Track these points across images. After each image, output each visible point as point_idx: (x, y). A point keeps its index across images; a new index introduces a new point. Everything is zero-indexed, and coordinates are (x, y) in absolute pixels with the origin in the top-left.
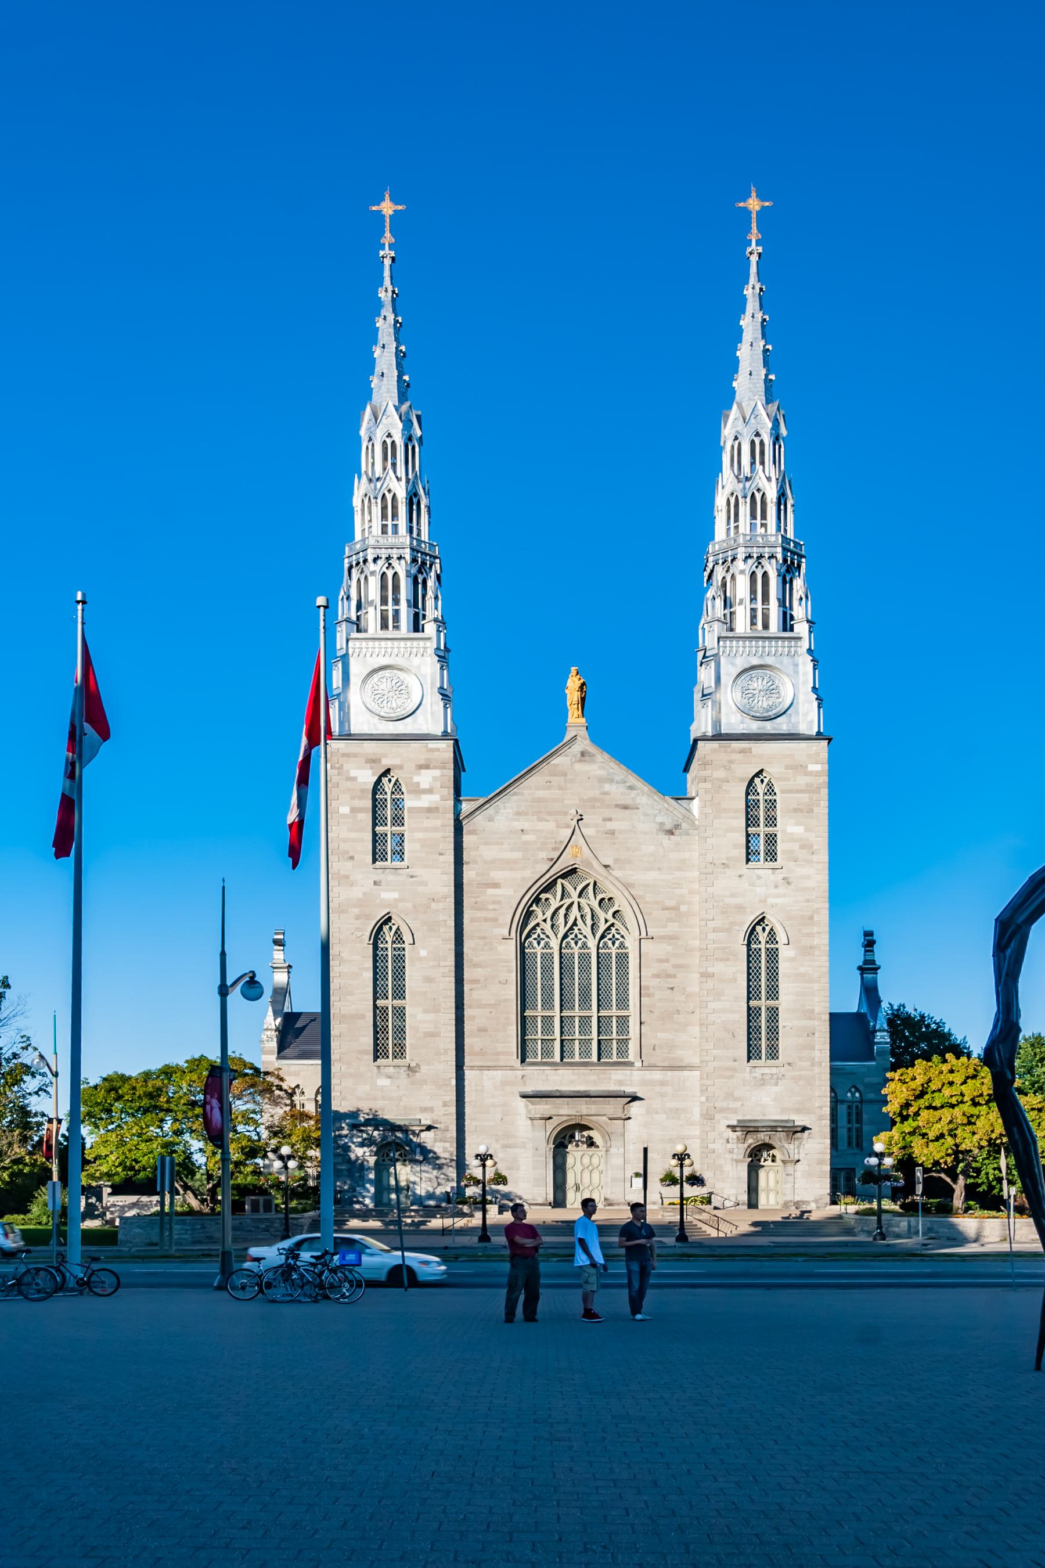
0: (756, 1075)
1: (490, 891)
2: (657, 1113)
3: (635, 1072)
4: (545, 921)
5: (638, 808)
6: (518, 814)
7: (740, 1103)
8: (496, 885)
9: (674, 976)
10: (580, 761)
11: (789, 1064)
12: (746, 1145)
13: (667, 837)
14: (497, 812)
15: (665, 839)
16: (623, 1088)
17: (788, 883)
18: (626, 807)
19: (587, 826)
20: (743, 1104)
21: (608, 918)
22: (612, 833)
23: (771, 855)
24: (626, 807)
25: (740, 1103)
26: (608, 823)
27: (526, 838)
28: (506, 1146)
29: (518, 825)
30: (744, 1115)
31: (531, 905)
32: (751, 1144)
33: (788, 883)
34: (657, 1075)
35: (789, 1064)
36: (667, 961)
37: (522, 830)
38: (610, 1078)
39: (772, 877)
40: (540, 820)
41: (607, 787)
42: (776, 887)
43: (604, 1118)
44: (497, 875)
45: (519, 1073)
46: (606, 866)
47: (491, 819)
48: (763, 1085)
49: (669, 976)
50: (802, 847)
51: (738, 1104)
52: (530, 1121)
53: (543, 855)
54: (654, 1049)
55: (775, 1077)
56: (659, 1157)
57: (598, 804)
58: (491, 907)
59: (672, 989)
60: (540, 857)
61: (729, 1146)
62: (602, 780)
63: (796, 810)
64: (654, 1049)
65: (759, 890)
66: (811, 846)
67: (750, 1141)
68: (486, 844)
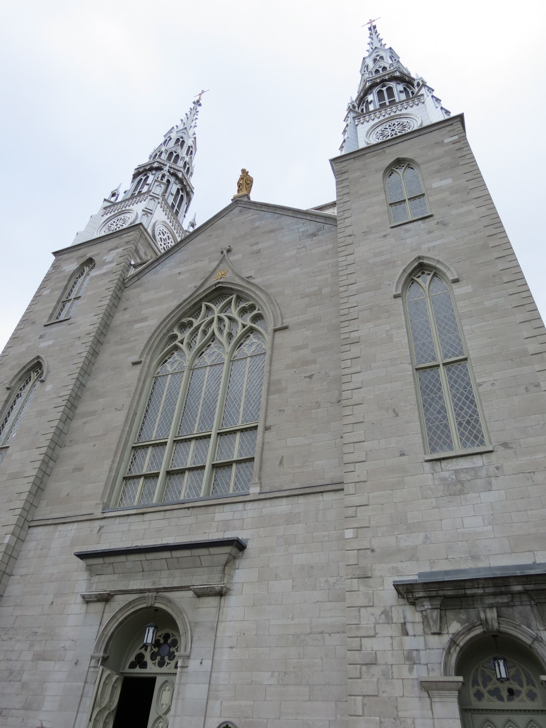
0: (446, 474)
2: (277, 577)
3: (249, 506)
7: (422, 535)
9: (314, 362)
11: (505, 445)
12: (446, 639)
20: (426, 537)
21: (245, 323)
22: (258, 252)
25: (422, 535)
27: (181, 277)
28: (40, 657)
29: (177, 271)
30: (432, 562)
31: (171, 329)
32: (457, 635)
35: (505, 445)
36: (305, 346)
37: (179, 273)
38: (213, 520)
43: (190, 594)
48: (461, 492)
49: (306, 363)
51: (417, 539)
52: (85, 606)
53: (193, 285)
54: (281, 463)
55: (483, 473)
56: (274, 681)
58: (132, 339)
59: (310, 377)
60: (189, 287)
61: (409, 643)
64: (281, 463)
67: (455, 627)
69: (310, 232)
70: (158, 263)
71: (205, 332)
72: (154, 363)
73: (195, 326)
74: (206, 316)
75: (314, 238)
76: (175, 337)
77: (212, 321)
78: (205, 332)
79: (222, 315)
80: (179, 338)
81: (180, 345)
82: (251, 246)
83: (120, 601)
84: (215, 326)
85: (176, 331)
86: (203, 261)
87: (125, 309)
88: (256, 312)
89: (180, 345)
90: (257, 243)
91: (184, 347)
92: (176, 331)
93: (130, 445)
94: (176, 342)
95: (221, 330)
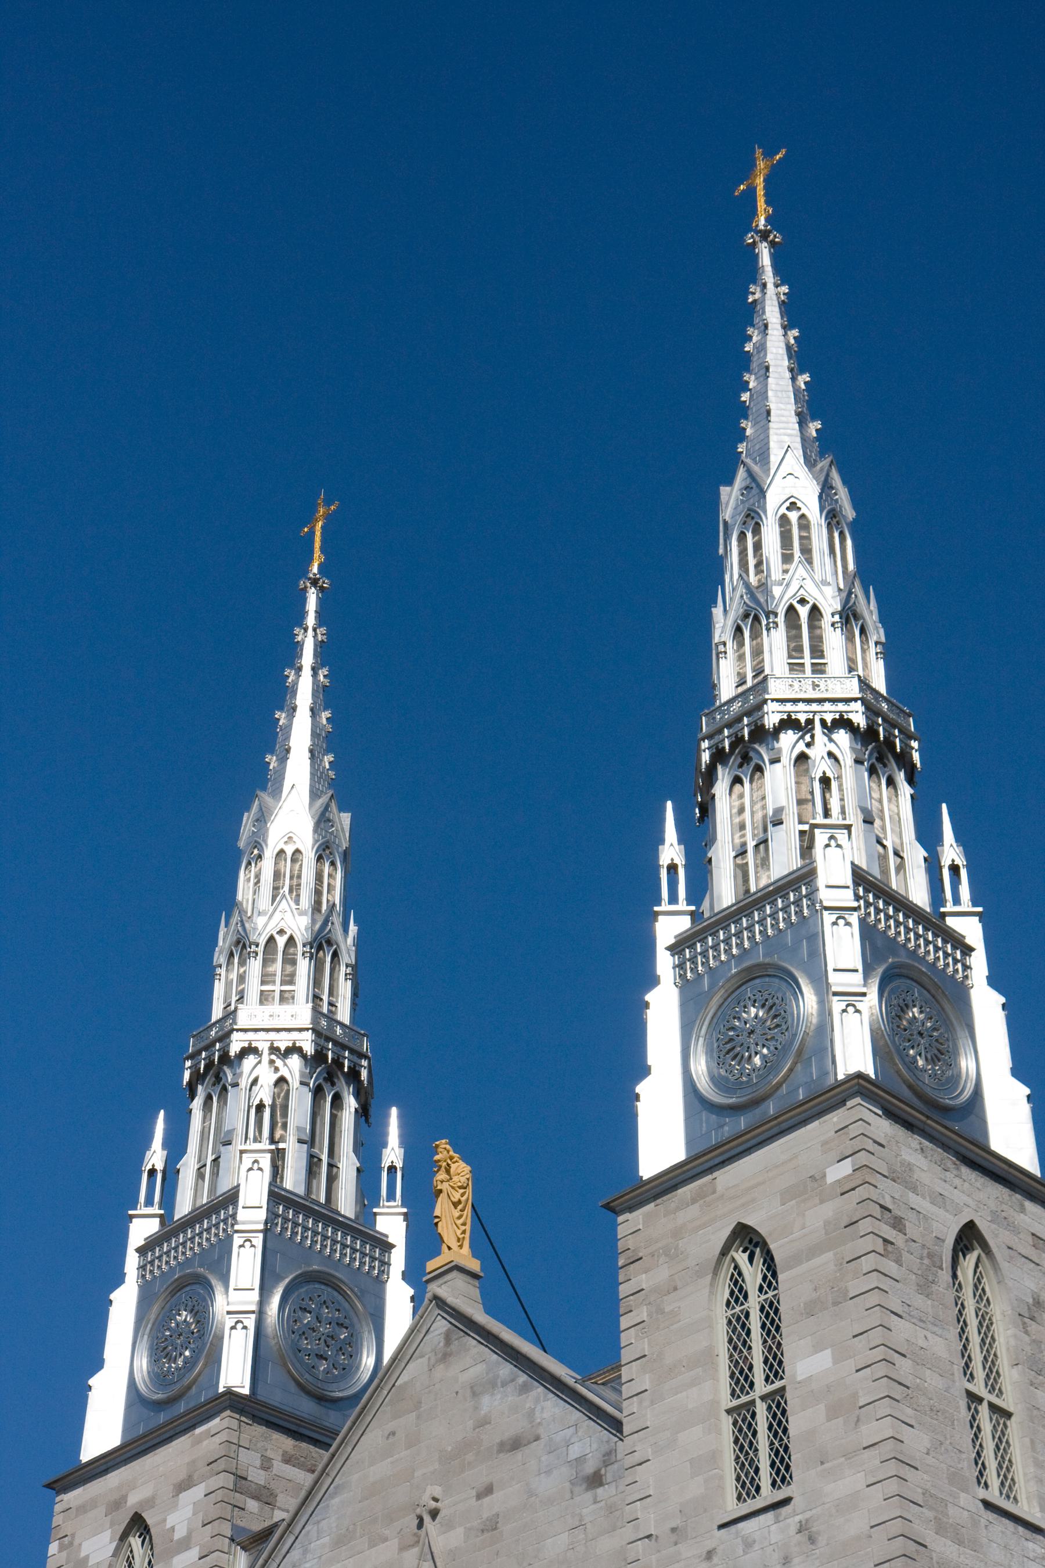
6: (339, 1542)
13: (589, 1495)
14: (305, 1552)
15: (587, 1506)
17: (812, 1540)
19: (449, 1526)
22: (491, 1526)
23: (782, 1473)
24: (515, 1445)
26: (487, 1500)
33: (812, 1540)
39: (776, 1535)
40: (372, 1544)
50: (833, 1413)
57: (470, 1457)
62: (475, 1392)
63: (810, 1310)
70: (293, 1538)
75: (600, 1491)
82: (479, 1497)
86: (386, 1540)
90: (489, 1490)
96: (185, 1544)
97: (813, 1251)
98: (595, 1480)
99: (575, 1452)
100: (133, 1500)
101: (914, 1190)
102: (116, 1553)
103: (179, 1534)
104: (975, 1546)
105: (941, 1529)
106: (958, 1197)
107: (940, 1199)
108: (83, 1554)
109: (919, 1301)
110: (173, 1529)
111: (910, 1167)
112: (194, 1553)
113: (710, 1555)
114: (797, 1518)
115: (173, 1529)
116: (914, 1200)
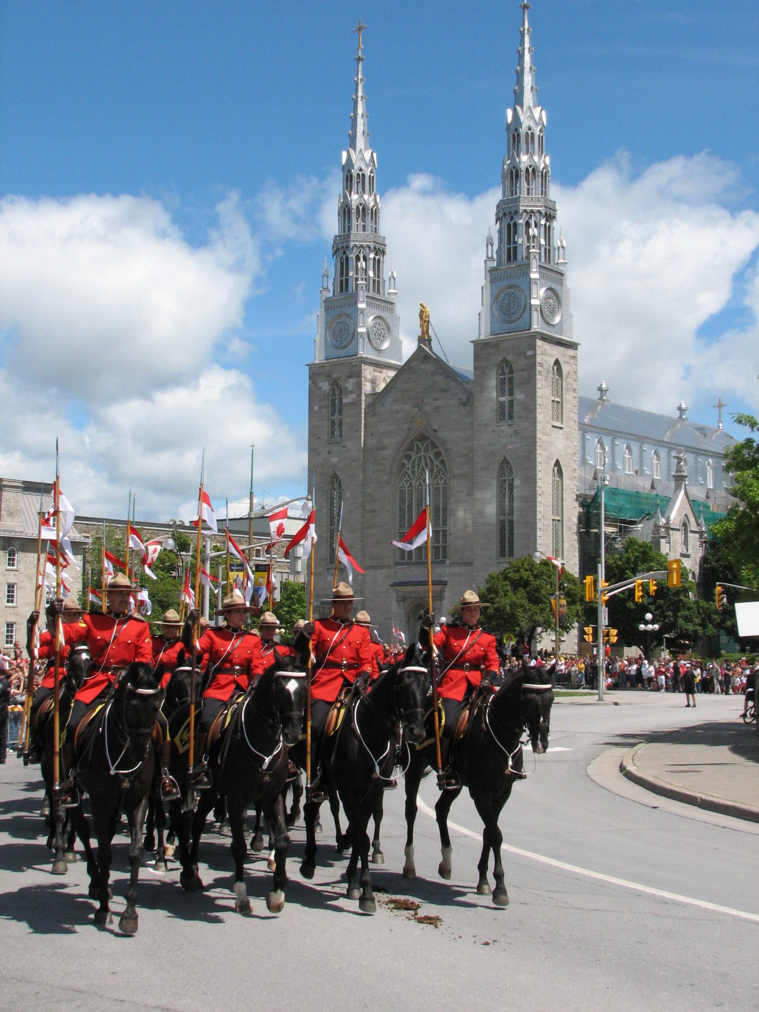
1: (382, 452)
3: (447, 568)
4: (408, 469)
5: (449, 391)
8: (385, 448)
10: (423, 362)
16: (441, 579)
18: (443, 390)
22: (437, 408)
23: (511, 417)
24: (443, 390)
27: (400, 415)
33: (517, 434)
34: (457, 570)
37: (397, 411)
41: (435, 378)
42: (511, 437)
44: (386, 441)
45: (393, 570)
46: (435, 430)
47: (383, 405)
50: (524, 408)
53: (406, 426)
65: (502, 440)
66: (528, 407)
68: (381, 422)
69: (464, 400)
71: (419, 464)
72: (397, 482)
73: (413, 458)
74: (416, 454)
75: (466, 408)
76: (404, 465)
77: (420, 460)
78: (419, 464)
79: (425, 454)
80: (407, 467)
81: (407, 470)
83: (408, 601)
84: (423, 462)
85: (404, 461)
87: (372, 435)
88: (440, 458)
89: (407, 470)
90: (436, 400)
91: (409, 472)
92: (404, 461)
93: (397, 531)
94: (405, 469)
95: (426, 464)
96: (351, 392)
97: (522, 370)
98: (465, 405)
99: (460, 396)
100: (334, 376)
101: (545, 355)
102: (330, 389)
103: (350, 389)
104: (550, 435)
105: (544, 434)
106: (555, 353)
107: (551, 356)
108: (320, 386)
109: (545, 383)
110: (347, 388)
111: (545, 350)
112: (354, 396)
113: (493, 431)
114: (514, 429)
115: (347, 388)
116: (546, 358)
